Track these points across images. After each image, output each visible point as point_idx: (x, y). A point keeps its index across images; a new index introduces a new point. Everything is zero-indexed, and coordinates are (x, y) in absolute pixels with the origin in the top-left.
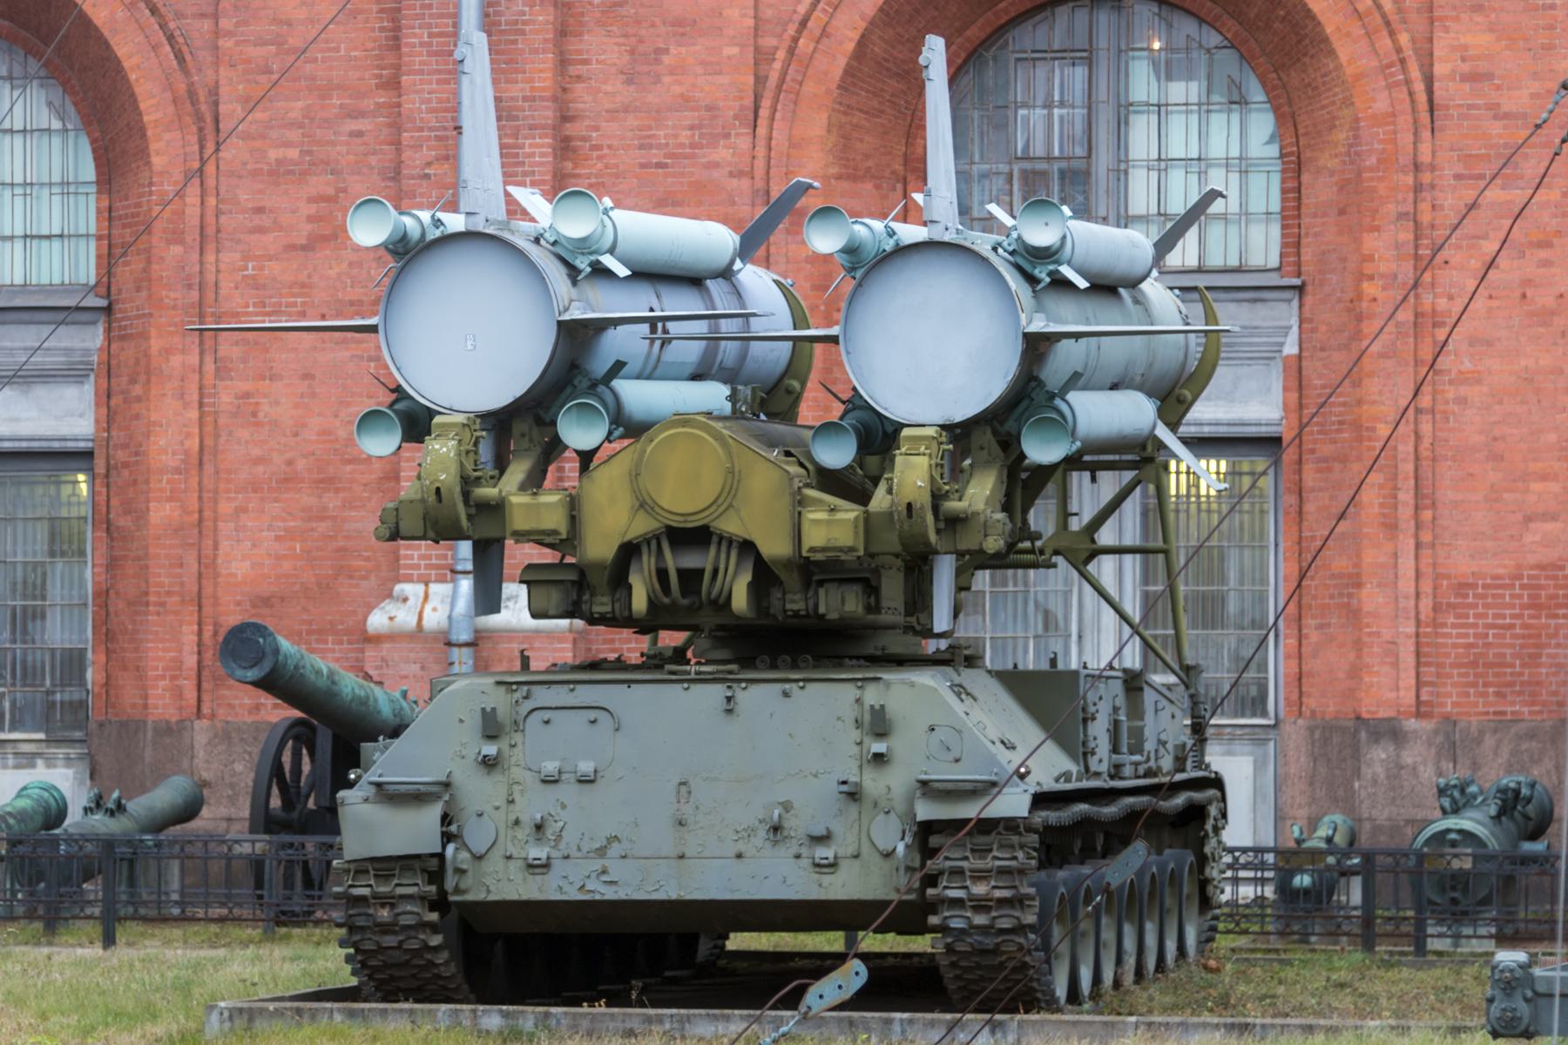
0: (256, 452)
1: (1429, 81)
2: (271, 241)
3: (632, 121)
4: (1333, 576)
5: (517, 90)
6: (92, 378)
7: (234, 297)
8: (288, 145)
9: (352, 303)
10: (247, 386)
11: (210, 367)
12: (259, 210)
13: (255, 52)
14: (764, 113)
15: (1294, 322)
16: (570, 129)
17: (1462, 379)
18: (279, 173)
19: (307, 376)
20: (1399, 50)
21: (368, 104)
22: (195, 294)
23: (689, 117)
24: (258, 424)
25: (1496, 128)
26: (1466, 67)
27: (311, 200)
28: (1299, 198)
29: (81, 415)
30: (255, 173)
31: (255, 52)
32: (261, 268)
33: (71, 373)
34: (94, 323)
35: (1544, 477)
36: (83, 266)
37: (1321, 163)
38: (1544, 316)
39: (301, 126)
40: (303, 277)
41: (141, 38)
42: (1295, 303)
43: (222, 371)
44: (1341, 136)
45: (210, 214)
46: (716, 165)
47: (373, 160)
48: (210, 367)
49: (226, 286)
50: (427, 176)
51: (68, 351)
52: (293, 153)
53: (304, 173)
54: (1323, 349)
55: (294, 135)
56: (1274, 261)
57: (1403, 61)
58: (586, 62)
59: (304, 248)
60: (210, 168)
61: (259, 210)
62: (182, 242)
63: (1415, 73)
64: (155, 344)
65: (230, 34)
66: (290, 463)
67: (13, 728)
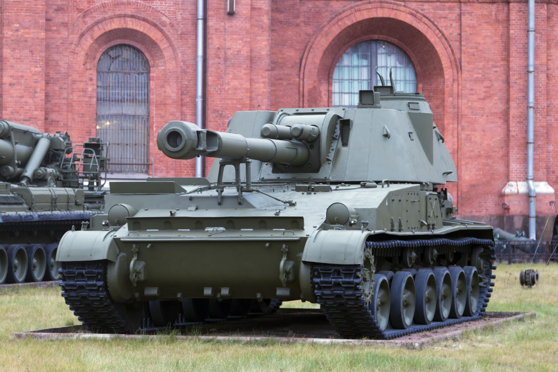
0: (471, 149)
2: (475, 97)
5: (538, 62)
7: (465, 110)
8: (479, 74)
9: (495, 113)
10: (468, 133)
11: (460, 128)
12: (472, 90)
13: (470, 50)
16: (550, 72)
18: (476, 80)
19: (484, 131)
21: (499, 64)
22: (456, 110)
24: (472, 142)
27: (485, 87)
31: (470, 50)
39: (482, 69)
40: (482, 106)
41: (442, 46)
43: (463, 129)
45: (460, 90)
47: (500, 78)
48: (460, 128)
49: (463, 108)
50: (516, 83)
52: (480, 76)
53: (483, 81)
55: (480, 71)
58: (551, 56)
59: (483, 99)
60: (460, 79)
61: (472, 90)
62: (452, 97)
64: (446, 122)
65: (464, 46)
66: (479, 152)
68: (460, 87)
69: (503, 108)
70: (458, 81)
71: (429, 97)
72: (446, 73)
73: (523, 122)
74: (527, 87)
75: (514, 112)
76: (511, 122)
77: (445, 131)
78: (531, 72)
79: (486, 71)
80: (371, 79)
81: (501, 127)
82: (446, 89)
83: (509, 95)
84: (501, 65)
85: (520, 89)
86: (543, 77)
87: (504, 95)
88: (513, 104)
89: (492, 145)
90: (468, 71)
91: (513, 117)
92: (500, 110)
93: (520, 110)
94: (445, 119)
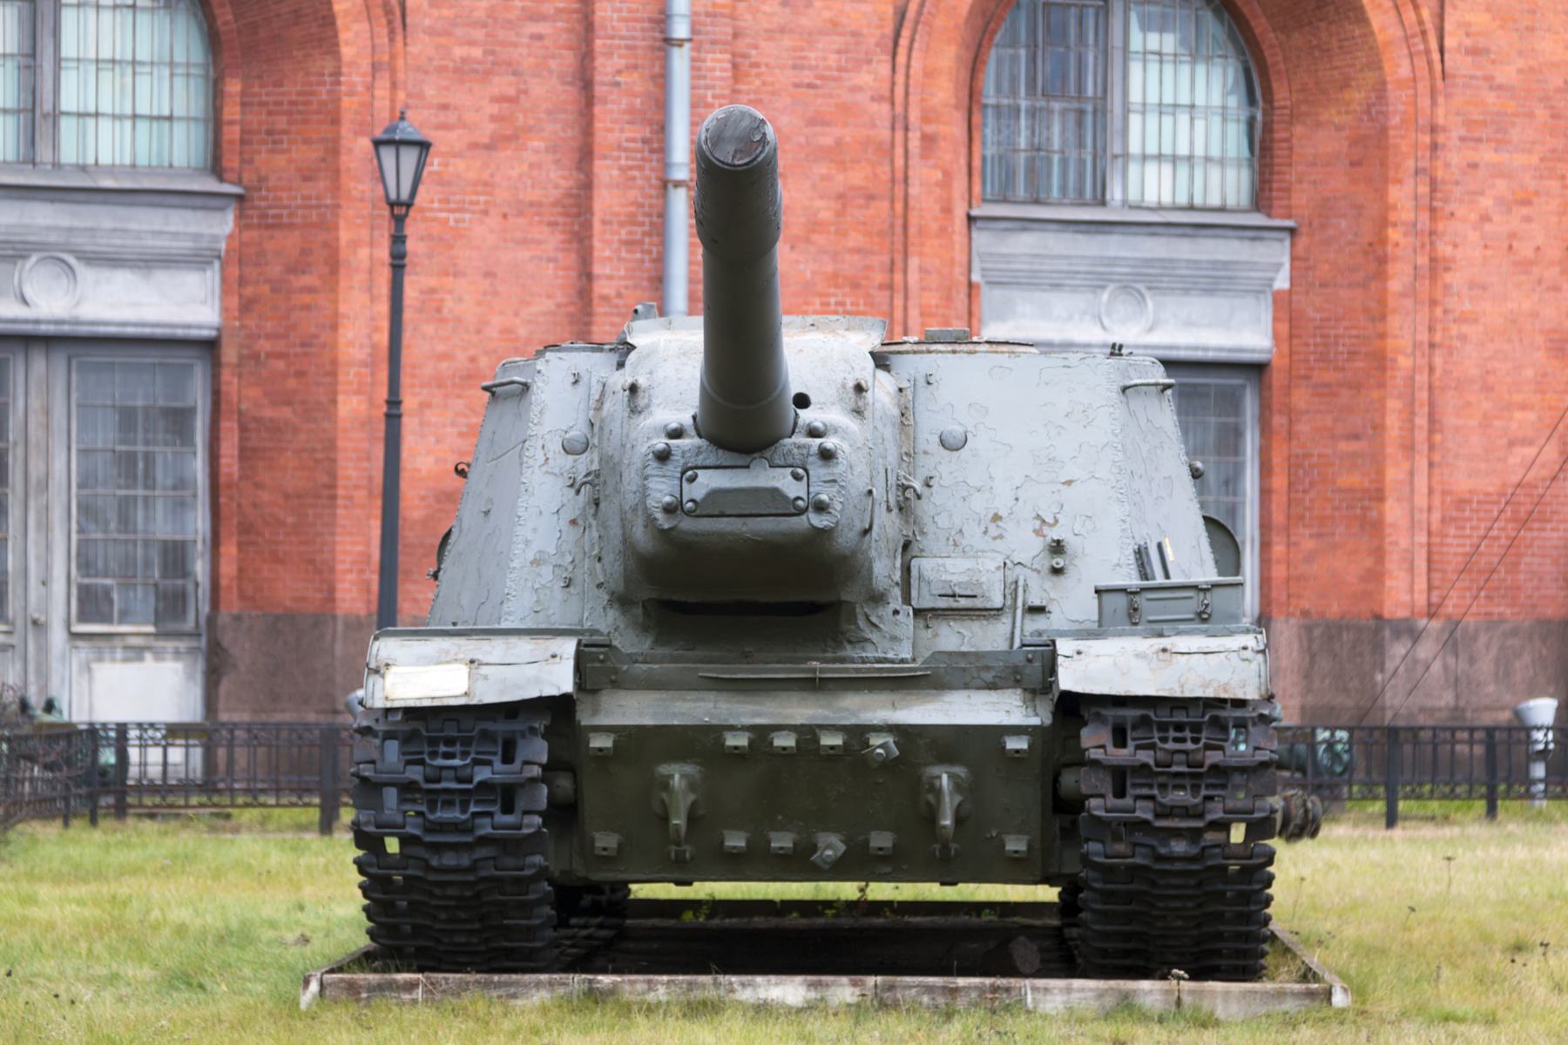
0: (441, 347)
1: (1442, 51)
3: (787, 42)
4: (1340, 490)
6: (217, 265)
8: (472, 43)
9: (532, 204)
10: (432, 282)
12: (444, 107)
14: (904, 42)
15: (1286, 260)
16: (741, 45)
17: (1463, 319)
18: (462, 72)
19: (489, 274)
20: (1421, 22)
23: (838, 41)
24: (443, 321)
25: (1491, 98)
26: (1468, 42)
28: (1291, 149)
29: (204, 302)
30: (441, 70)
32: (446, 165)
33: (196, 260)
34: (222, 209)
35: (1524, 407)
36: (183, 147)
37: (1324, 117)
38: (1524, 266)
39: (485, 25)
40: (485, 176)
42: (1287, 243)
44: (1357, 96)
46: (856, 89)
47: (553, 64)
50: (618, 84)
51: (196, 237)
52: (477, 52)
54: (1323, 285)
55: (479, 34)
56: (1245, 200)
57: (1424, 33)
59: (489, 147)
60: (400, 62)
61: (444, 107)
63: (1434, 45)
64: (344, 236)
66: (473, 359)
67: (121, 622)
68: (401, 95)
69: (563, 183)
70: (393, 70)
71: (269, 132)
72: (344, 36)
73: (641, 242)
74: (662, 104)
75: (607, 201)
76: (597, 243)
77: (342, 271)
78: (680, 43)
79: (502, 34)
80: (33, 55)
81: (555, 260)
82: (346, 101)
83: (587, 131)
84: (559, 11)
85: (631, 110)
86: (718, 63)
87: (570, 133)
88: (605, 171)
89: (523, 332)
90: (431, 32)
91: (604, 222)
92: (555, 193)
93: (633, 194)
94: (342, 223)
